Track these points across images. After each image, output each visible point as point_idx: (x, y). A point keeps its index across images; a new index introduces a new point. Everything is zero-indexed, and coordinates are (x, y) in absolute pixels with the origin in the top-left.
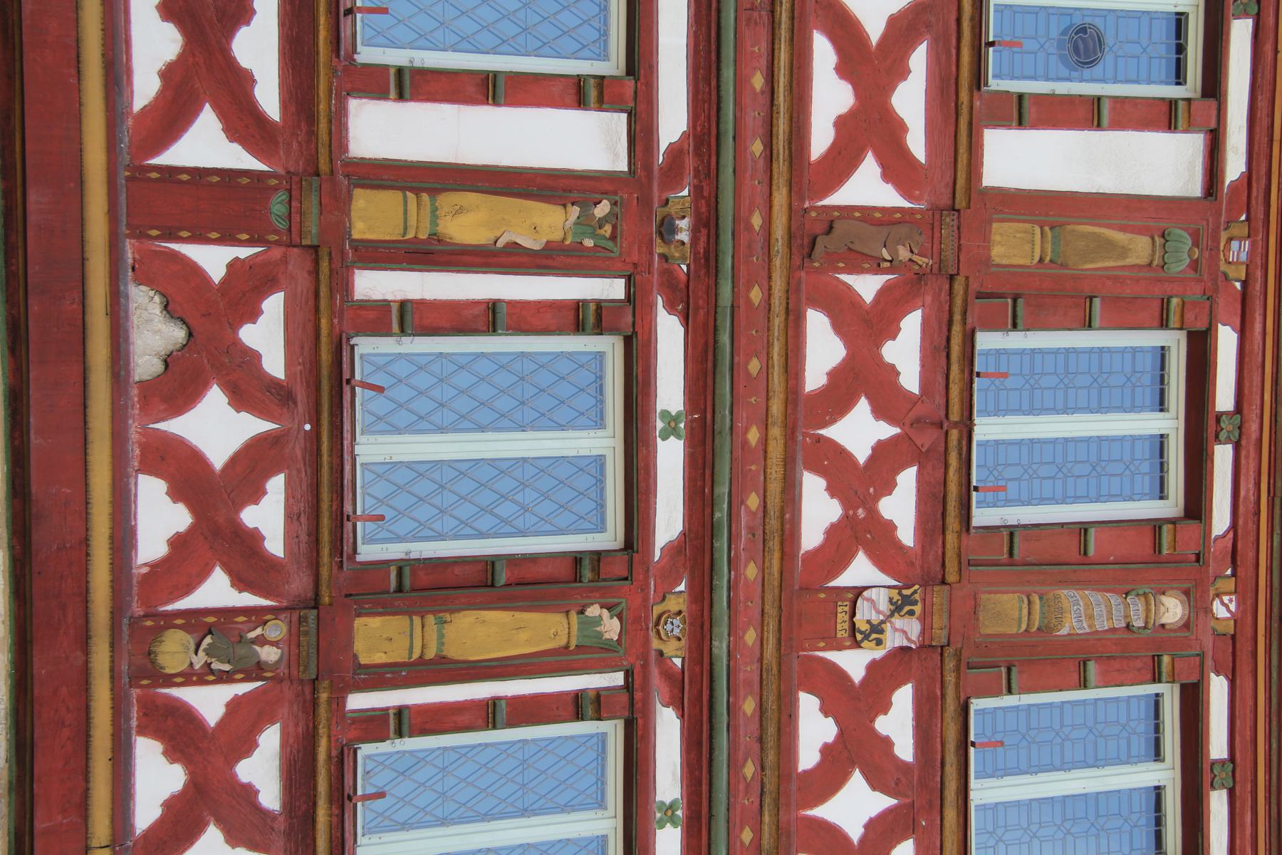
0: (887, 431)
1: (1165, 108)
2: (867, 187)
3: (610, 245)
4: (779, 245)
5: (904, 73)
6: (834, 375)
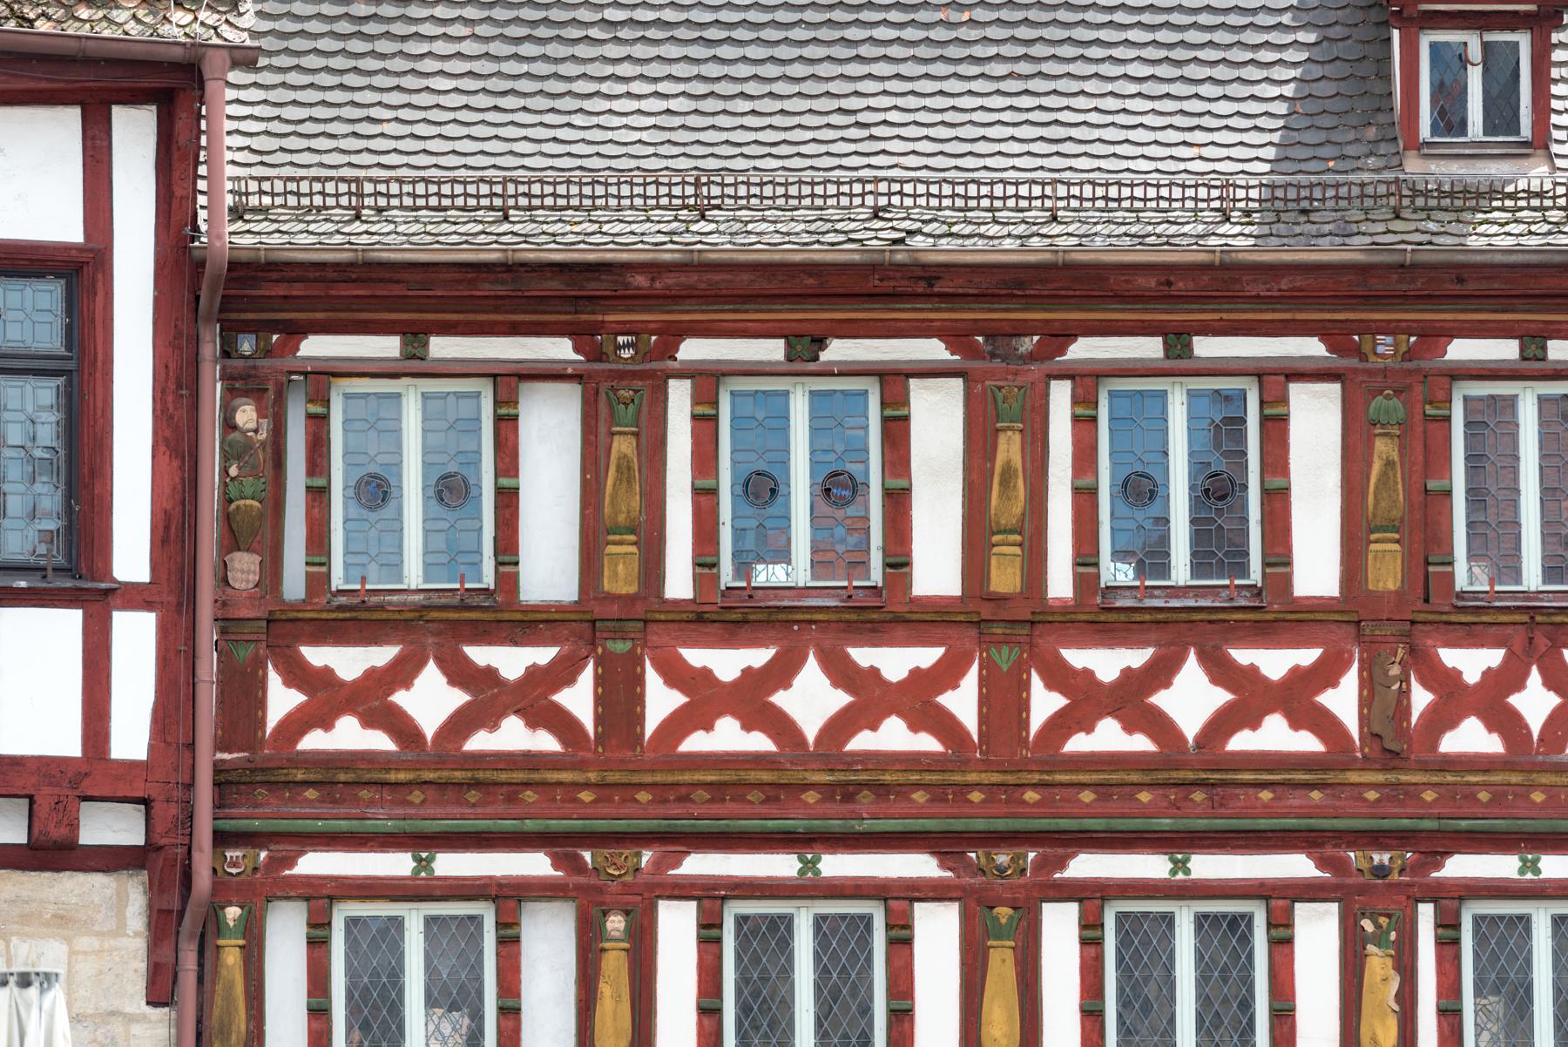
0: (1535, 678)
1: (1270, 424)
2: (1342, 701)
3: (1394, 919)
4: (1391, 777)
5: (1253, 670)
6: (1491, 728)
